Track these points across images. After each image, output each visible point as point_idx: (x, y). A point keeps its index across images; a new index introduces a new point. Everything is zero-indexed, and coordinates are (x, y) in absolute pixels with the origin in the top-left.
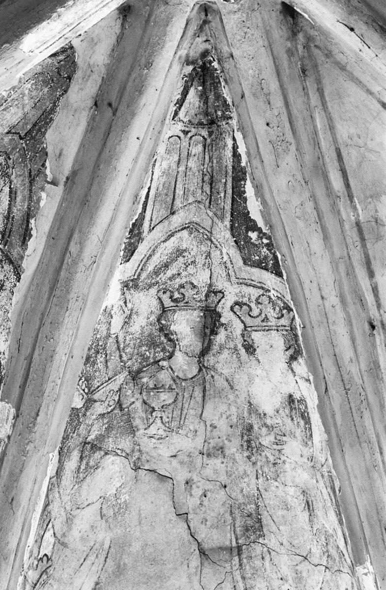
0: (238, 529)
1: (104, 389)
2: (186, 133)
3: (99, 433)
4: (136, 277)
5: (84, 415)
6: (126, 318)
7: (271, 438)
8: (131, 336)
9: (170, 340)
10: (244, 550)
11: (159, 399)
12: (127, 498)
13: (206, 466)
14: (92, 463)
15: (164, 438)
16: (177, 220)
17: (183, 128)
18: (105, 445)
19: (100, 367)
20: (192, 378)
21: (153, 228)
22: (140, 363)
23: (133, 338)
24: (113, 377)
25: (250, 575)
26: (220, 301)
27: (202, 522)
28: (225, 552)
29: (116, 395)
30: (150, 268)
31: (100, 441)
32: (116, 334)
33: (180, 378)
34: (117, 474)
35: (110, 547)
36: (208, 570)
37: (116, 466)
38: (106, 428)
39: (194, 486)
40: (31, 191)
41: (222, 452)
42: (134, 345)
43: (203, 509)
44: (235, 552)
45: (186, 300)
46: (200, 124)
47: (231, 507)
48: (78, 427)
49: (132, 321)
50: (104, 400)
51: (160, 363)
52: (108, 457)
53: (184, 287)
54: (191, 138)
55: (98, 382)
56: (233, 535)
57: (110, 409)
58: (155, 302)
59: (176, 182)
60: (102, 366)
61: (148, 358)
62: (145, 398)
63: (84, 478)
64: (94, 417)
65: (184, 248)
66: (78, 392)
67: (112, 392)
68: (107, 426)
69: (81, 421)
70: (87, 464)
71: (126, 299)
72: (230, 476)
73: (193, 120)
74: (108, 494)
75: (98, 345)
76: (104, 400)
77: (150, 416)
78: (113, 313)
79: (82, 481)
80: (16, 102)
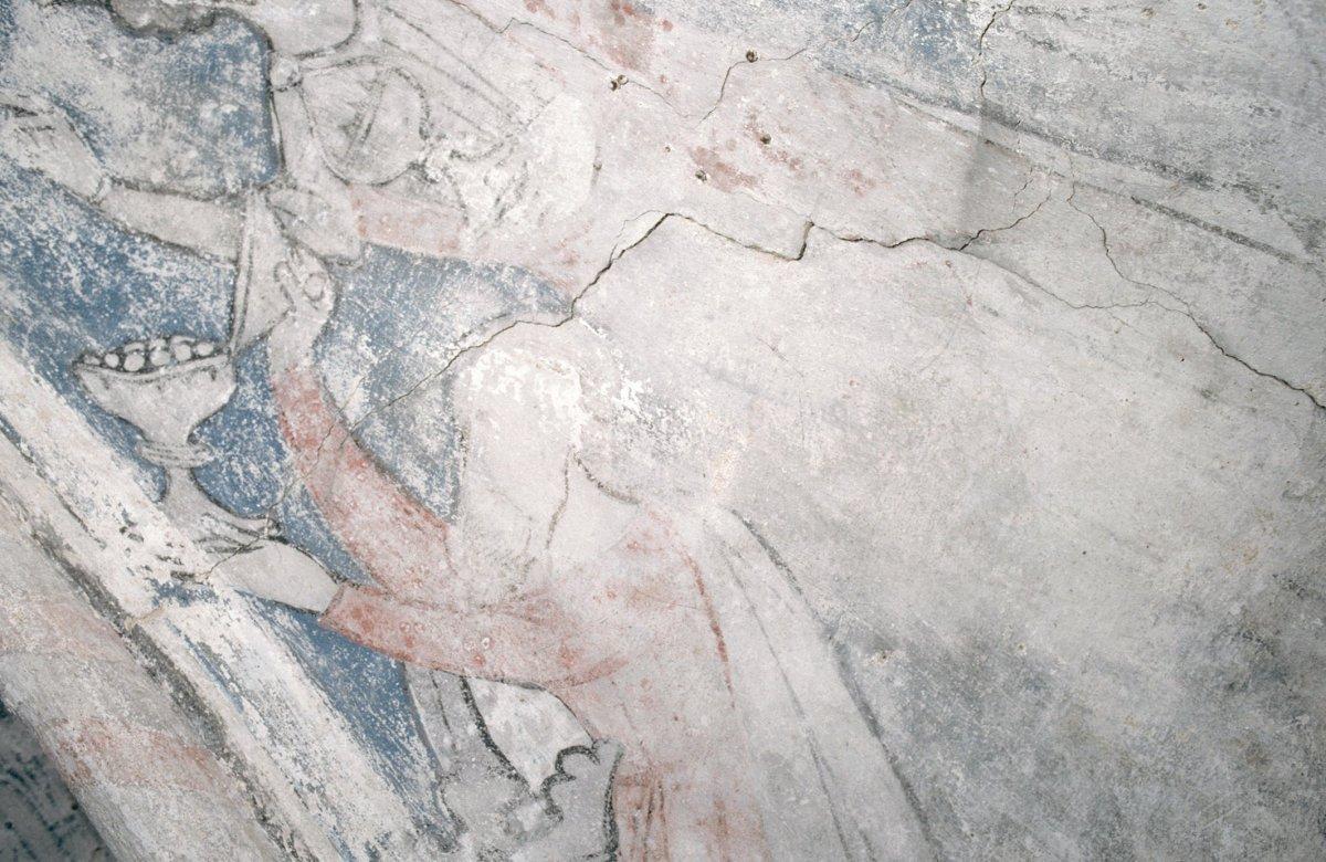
0: (918, 82)
1: (252, 289)
3: (365, 372)
5: (268, 392)
6: (72, 129)
8: (143, 137)
9: (211, 20)
10: (1000, 99)
11: (392, 137)
12: (637, 387)
13: (667, 86)
14: (433, 445)
15: (526, 177)
18: (419, 372)
19: (172, 274)
22: (249, 144)
23: (152, 133)
24: (239, 246)
25: (1106, 126)
27: (857, 189)
28: (991, 170)
29: (301, 262)
31: (392, 383)
32: (107, 180)
34: (540, 378)
35: (749, 526)
36: (1036, 257)
37: (509, 370)
38: (369, 344)
39: (725, 157)
41: (629, 11)
42: (178, 137)
43: (811, 163)
44: (1004, 137)
47: (831, 68)
48: (280, 433)
49: (92, 114)
50: (283, 305)
51: (276, 82)
52: (459, 384)
55: (214, 298)
56: (937, 111)
57: (328, 303)
60: (175, 265)
61: (242, 114)
62: (367, 177)
63: (455, 494)
64: (307, 362)
66: (177, 382)
67: (283, 271)
68: (366, 338)
69: (270, 411)
70: (423, 459)
71: (8, 106)
72: (719, 20)
74: (575, 440)
75: (99, 248)
76: (283, 305)
77: (432, 190)
78: (25, 164)
79: (454, 505)
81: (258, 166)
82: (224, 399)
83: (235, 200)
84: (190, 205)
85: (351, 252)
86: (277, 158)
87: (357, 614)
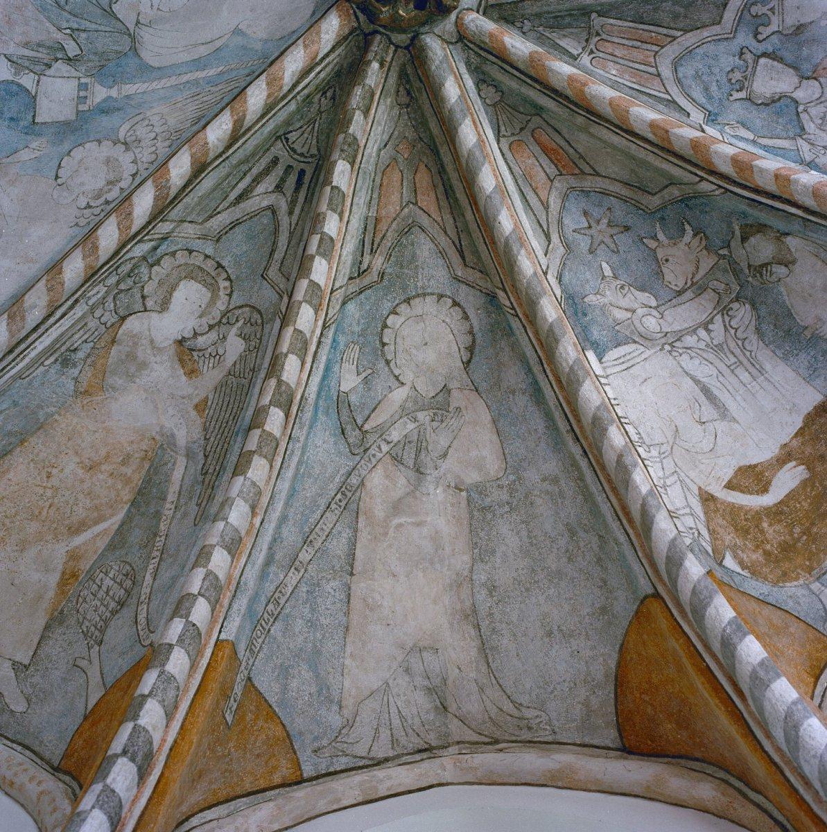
9: (780, 99)
16: (666, 72)
17: (587, 54)
26: (750, 51)
30: (703, 101)
40: (605, 177)
46: (587, 41)
51: (799, 111)
53: (731, 79)
73: (583, 46)
81: (799, 131)
83: (794, 139)
86: (803, 129)
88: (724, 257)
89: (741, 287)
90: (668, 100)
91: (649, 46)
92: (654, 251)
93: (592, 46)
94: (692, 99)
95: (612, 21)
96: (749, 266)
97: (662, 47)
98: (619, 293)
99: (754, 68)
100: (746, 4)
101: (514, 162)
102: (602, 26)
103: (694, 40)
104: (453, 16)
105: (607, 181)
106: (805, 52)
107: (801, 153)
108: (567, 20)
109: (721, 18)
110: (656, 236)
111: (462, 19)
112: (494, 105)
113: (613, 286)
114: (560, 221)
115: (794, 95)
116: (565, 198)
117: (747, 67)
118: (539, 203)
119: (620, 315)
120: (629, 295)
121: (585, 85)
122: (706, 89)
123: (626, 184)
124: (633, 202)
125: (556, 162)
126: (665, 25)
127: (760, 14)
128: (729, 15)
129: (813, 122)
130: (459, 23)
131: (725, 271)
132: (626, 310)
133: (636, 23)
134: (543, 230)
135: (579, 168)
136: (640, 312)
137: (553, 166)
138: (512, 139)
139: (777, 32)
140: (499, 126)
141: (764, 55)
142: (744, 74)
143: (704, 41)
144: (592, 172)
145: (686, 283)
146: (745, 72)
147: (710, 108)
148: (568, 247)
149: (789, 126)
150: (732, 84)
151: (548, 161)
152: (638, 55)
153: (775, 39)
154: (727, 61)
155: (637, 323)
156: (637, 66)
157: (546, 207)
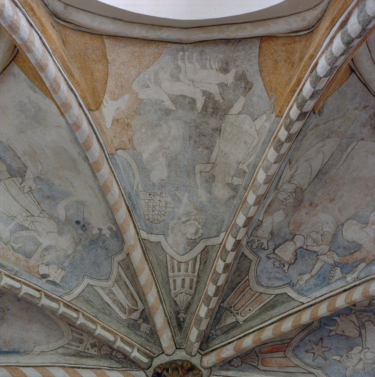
2: (237, 313)
4: (288, 285)
7: (288, 201)
9: (296, 253)
16: (261, 290)
17: (237, 315)
20: (301, 235)
21: (270, 294)
26: (270, 254)
33: (304, 237)
41: (311, 204)
45: (279, 263)
46: (231, 312)
50: (332, 258)
53: (277, 267)
54: (237, 311)
57: (334, 253)
58: (290, 270)
59: (252, 301)
62: (321, 242)
65: (267, 279)
76: (332, 258)
78: (304, 282)
80: (277, 364)
81: (315, 254)
82: (340, 269)
83: (318, 259)
84: (316, 265)
85: (329, 247)
86: (315, 252)
87: (369, 261)
88: (355, 313)
89: (371, 312)
90: (275, 297)
91: (246, 290)
92: (337, 334)
93: (235, 312)
94: (278, 287)
95: (228, 299)
96: (366, 307)
97: (249, 285)
98: (350, 359)
99: (277, 256)
100: (250, 249)
101: (271, 368)
102: (228, 304)
103: (253, 273)
104: (202, 369)
105: (297, 336)
106: (282, 234)
107: (327, 262)
108: (218, 315)
109: (250, 259)
110: (331, 330)
111: (205, 367)
112: (242, 362)
113: (346, 360)
114: (307, 364)
115: (298, 246)
116: (296, 355)
117: (276, 258)
118: (294, 368)
119: (360, 366)
120: (352, 356)
121: (260, 339)
122: (277, 278)
123: (302, 330)
124: (311, 331)
125: (278, 350)
126: (241, 280)
127: (257, 245)
128: (250, 256)
129: (314, 246)
130: (205, 368)
131: (361, 314)
132: (359, 362)
133: (233, 291)
134: (307, 373)
135: (285, 343)
136: (362, 356)
137: (280, 352)
138: (260, 362)
139: (268, 241)
140: (252, 365)
141: (274, 250)
142: (278, 261)
143: (255, 270)
144: (291, 340)
145: (358, 330)
146: (277, 260)
147: (287, 282)
148: (319, 368)
149: (311, 257)
150: (280, 267)
151: (277, 353)
152: (248, 296)
153: (269, 243)
154: (269, 264)
155: (368, 362)
156: (252, 299)
157: (297, 366)
